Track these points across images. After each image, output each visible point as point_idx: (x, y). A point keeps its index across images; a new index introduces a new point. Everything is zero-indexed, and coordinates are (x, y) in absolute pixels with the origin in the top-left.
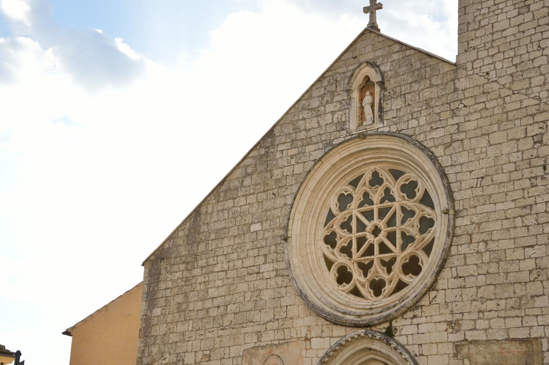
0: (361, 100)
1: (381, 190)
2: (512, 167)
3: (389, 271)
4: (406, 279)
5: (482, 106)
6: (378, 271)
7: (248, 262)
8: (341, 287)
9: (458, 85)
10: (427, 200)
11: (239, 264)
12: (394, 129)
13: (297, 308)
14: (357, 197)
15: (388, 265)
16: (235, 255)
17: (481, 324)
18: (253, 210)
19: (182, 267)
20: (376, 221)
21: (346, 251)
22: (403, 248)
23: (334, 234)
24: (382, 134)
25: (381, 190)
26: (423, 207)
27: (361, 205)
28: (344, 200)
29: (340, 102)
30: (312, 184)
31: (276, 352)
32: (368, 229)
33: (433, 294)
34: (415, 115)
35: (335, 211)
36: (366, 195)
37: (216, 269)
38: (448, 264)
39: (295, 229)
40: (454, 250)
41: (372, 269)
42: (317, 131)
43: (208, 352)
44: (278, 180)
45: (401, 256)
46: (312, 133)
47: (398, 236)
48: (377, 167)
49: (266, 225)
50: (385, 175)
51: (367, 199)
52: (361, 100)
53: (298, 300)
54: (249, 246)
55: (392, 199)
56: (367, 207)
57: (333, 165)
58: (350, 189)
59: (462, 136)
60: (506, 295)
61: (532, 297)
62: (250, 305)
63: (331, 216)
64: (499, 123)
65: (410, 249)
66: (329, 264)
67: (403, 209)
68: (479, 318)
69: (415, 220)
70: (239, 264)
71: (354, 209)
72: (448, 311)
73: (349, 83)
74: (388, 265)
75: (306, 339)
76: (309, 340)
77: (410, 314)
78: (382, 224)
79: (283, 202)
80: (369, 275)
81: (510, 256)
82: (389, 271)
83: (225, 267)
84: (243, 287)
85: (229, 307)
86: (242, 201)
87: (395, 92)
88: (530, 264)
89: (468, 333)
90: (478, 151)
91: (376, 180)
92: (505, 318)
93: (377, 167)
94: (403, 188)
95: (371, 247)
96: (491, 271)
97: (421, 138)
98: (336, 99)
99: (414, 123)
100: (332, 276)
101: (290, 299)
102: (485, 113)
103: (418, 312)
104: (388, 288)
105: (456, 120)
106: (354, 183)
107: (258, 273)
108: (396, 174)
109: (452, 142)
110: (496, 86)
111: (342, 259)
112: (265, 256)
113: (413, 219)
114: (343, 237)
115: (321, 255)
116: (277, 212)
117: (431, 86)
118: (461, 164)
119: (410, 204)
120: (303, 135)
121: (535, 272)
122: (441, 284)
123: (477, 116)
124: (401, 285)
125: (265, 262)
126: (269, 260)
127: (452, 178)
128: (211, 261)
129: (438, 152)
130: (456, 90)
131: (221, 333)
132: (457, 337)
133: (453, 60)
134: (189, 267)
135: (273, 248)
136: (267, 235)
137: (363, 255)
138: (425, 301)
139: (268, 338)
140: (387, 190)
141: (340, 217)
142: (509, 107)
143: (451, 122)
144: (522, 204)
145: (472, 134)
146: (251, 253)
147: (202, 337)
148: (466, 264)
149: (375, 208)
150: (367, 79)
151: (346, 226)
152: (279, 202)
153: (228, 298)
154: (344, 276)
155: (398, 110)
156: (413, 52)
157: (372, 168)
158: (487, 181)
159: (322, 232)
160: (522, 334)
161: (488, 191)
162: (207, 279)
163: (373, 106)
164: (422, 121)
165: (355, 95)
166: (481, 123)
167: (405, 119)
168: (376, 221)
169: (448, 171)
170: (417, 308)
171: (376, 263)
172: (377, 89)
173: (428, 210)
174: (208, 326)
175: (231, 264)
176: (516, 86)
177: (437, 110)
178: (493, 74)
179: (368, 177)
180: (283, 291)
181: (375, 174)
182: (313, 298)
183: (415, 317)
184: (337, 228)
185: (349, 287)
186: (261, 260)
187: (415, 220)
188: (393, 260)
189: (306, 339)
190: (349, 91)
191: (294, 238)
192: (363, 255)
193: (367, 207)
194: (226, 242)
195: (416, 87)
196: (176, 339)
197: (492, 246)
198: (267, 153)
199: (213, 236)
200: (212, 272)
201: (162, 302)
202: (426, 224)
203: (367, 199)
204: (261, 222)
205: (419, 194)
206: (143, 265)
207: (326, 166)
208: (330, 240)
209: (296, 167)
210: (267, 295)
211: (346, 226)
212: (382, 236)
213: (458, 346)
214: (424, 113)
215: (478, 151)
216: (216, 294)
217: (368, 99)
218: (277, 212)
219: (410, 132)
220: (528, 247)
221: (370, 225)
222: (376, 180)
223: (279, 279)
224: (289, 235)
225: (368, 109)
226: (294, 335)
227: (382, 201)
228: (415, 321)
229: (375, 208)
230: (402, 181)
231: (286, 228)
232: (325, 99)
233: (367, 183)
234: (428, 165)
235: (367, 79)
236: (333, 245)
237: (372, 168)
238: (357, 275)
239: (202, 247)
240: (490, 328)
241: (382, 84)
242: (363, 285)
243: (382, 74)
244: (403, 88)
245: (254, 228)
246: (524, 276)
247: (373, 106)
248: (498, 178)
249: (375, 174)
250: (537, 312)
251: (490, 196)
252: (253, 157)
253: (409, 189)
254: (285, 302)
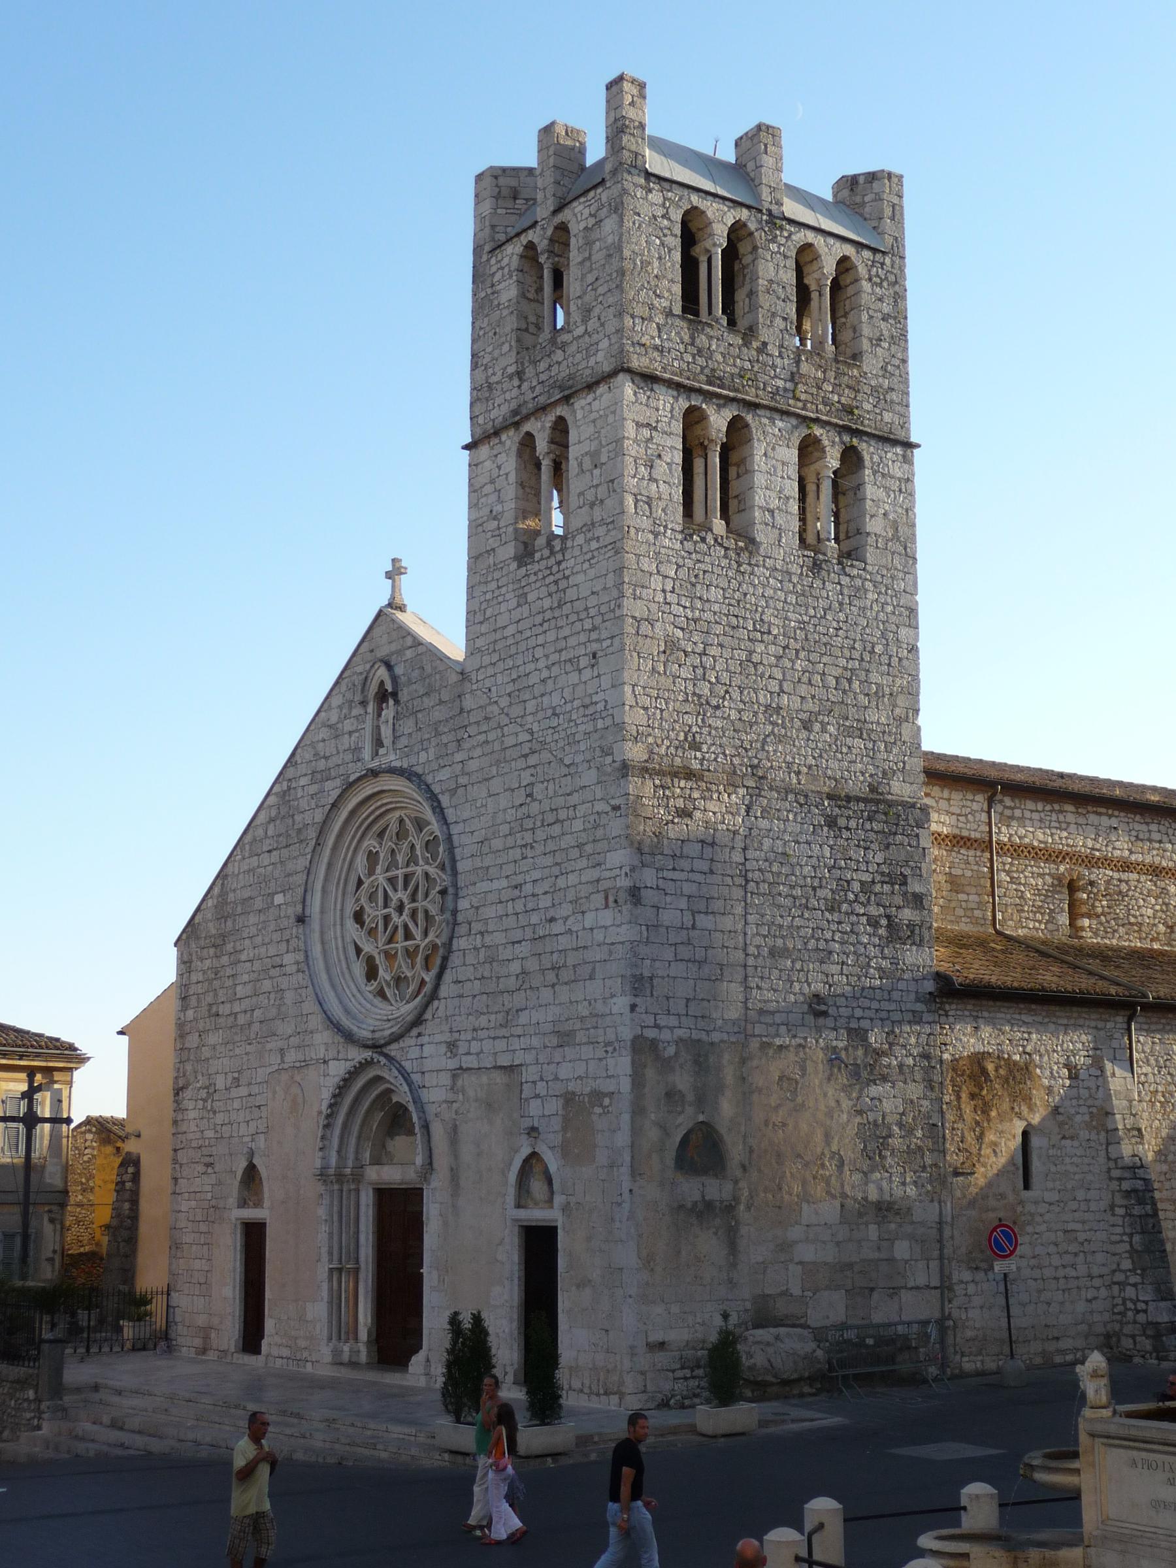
2: (505, 829)
17: (475, 1047)
21: (372, 932)
31: (298, 1078)
33: (436, 1003)
38: (450, 964)
43: (236, 1075)
48: (402, 813)
53: (317, 1008)
54: (272, 927)
57: (353, 813)
60: (496, 1009)
61: (517, 1011)
66: (358, 950)
68: (474, 1039)
72: (446, 1028)
75: (325, 1062)
77: (414, 1032)
81: (506, 953)
84: (267, 985)
88: (515, 967)
89: (464, 1058)
91: (401, 835)
92: (494, 1038)
96: (486, 974)
99: (423, 756)
100: (359, 969)
101: (310, 1006)
107: (281, 966)
114: (373, 913)
121: (520, 977)
126: (291, 948)
132: (452, 1064)
138: (428, 1015)
144: (514, 883)
147: (231, 1053)
148: (464, 965)
157: (397, 814)
158: (486, 849)
159: (350, 908)
160: (504, 1061)
161: (488, 861)
167: (416, 750)
170: (421, 1023)
174: (237, 1038)
179: (394, 828)
183: (419, 1035)
189: (325, 1062)
196: (208, 1055)
197: (488, 940)
198: (289, 788)
199: (239, 910)
200: (239, 962)
206: (176, 945)
213: (454, 1077)
214: (434, 742)
219: (419, 769)
220: (517, 942)
224: (307, 913)
228: (420, 1040)
233: (394, 837)
240: (482, 1051)
246: (512, 983)
248: (497, 844)
250: (519, 1031)
251: (488, 868)
252: (276, 794)
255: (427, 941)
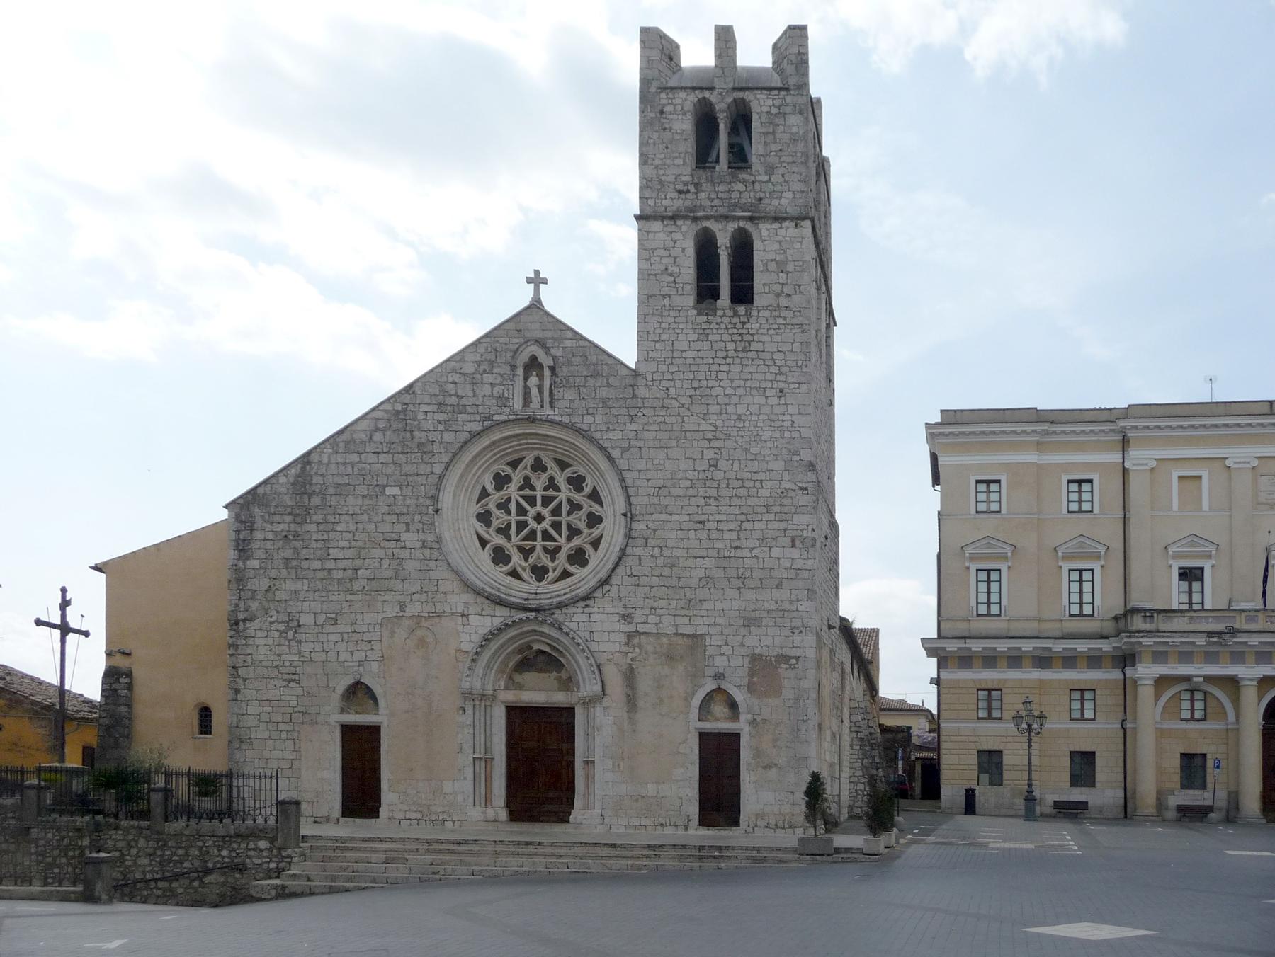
0: (526, 379)
1: (544, 477)
3: (553, 560)
4: (571, 569)
5: (661, 419)
6: (539, 556)
7: (388, 528)
8: (497, 568)
9: (637, 392)
10: (595, 496)
11: (371, 527)
12: (566, 419)
13: (450, 585)
14: (517, 478)
15: (553, 553)
16: (365, 517)
18: (389, 470)
19: (288, 518)
20: (539, 508)
22: (569, 539)
23: (488, 513)
24: (552, 422)
25: (544, 477)
26: (593, 504)
27: (520, 489)
28: (501, 481)
29: (502, 375)
30: (467, 457)
32: (530, 514)
33: (606, 588)
34: (591, 411)
35: (490, 488)
36: (527, 479)
37: (339, 528)
39: (446, 500)
40: (629, 551)
41: (535, 555)
42: (473, 400)
44: (420, 445)
45: (567, 548)
46: (464, 401)
47: (564, 527)
49: (407, 491)
50: (549, 463)
51: (527, 484)
52: (526, 379)
55: (558, 489)
56: (527, 492)
57: (493, 443)
58: (509, 470)
59: (640, 444)
62: (389, 573)
63: (484, 494)
64: (678, 439)
65: (577, 542)
67: (569, 500)
69: (582, 514)
70: (371, 527)
71: (512, 490)
73: (513, 357)
74: (553, 553)
76: (467, 616)
77: (582, 604)
78: (546, 512)
79: (429, 470)
80: (531, 561)
82: (553, 560)
83: (352, 528)
85: (359, 572)
86: (373, 458)
87: (568, 382)
90: (656, 462)
91: (539, 466)
93: (542, 454)
94: (570, 480)
95: (533, 532)
97: (597, 435)
98: (495, 371)
102: (663, 427)
103: (590, 602)
104: (551, 575)
105: (634, 427)
106: (514, 464)
108: (563, 465)
109: (630, 447)
110: (676, 404)
111: (499, 540)
112: (408, 524)
113: (581, 513)
115: (473, 532)
116: (422, 479)
117: (609, 385)
118: (639, 471)
119: (578, 498)
120: (453, 400)
122: (614, 580)
123: (655, 427)
124: (566, 574)
125: (408, 531)
127: (629, 482)
128: (331, 518)
129: (616, 454)
130: (634, 396)
131: (350, 597)
133: (633, 366)
134: (299, 519)
135: (417, 517)
136: (408, 502)
137: (523, 540)
138: (598, 594)
139: (412, 610)
140: (552, 479)
141: (496, 497)
142: (687, 427)
143: (630, 427)
145: (651, 444)
146: (387, 518)
149: (539, 494)
150: (534, 359)
151: (503, 506)
152: (424, 469)
153: (358, 563)
154: (500, 556)
155: (572, 401)
156: (587, 344)
157: (536, 453)
159: (475, 509)
162: (326, 537)
163: (540, 388)
164: (599, 419)
165: (520, 372)
166: (660, 435)
168: (539, 508)
169: (627, 475)
171: (539, 549)
172: (547, 373)
173: (597, 507)
175: (360, 526)
176: (695, 409)
177: (615, 412)
178: (672, 391)
179: (529, 461)
180: (432, 564)
181: (538, 459)
182: (469, 575)
183: (587, 606)
184: (492, 507)
185: (507, 568)
186: (402, 527)
187: (582, 514)
188: (558, 549)
190: (513, 367)
191: (444, 510)
192: (523, 540)
193: (527, 492)
194: (350, 500)
195: (591, 382)
201: (260, 554)
202: (594, 520)
203: (527, 484)
204: (401, 487)
205: (587, 490)
207: (485, 442)
208: (484, 518)
209: (445, 434)
210: (411, 566)
211: (503, 506)
212: (546, 524)
215: (656, 462)
216: (340, 556)
217: (533, 380)
218: (422, 479)
221: (532, 512)
222: (539, 466)
223: (427, 552)
225: (535, 391)
226: (447, 608)
227: (545, 489)
228: (587, 610)
229: (539, 494)
230: (568, 472)
231: (435, 498)
232: (482, 368)
234: (604, 464)
235: (534, 359)
236: (488, 524)
237: (536, 453)
238: (516, 559)
239: (316, 500)
241: (552, 369)
242: (524, 569)
243: (554, 358)
244: (578, 380)
245: (389, 491)
247: (540, 388)
249: (538, 459)
252: (386, 411)
253: (577, 483)
254: (434, 575)
255: (571, 545)
